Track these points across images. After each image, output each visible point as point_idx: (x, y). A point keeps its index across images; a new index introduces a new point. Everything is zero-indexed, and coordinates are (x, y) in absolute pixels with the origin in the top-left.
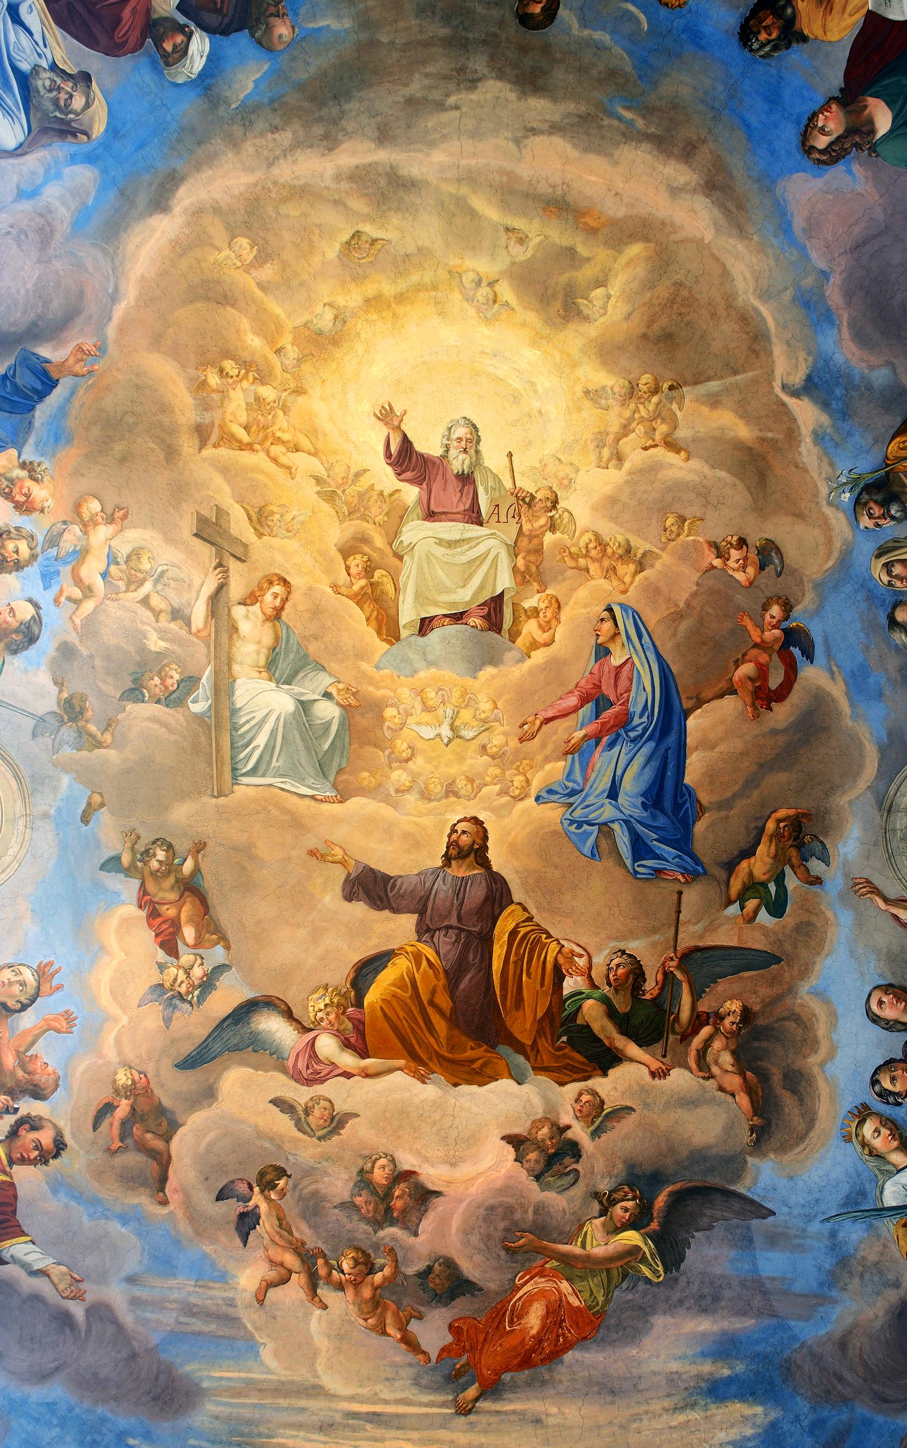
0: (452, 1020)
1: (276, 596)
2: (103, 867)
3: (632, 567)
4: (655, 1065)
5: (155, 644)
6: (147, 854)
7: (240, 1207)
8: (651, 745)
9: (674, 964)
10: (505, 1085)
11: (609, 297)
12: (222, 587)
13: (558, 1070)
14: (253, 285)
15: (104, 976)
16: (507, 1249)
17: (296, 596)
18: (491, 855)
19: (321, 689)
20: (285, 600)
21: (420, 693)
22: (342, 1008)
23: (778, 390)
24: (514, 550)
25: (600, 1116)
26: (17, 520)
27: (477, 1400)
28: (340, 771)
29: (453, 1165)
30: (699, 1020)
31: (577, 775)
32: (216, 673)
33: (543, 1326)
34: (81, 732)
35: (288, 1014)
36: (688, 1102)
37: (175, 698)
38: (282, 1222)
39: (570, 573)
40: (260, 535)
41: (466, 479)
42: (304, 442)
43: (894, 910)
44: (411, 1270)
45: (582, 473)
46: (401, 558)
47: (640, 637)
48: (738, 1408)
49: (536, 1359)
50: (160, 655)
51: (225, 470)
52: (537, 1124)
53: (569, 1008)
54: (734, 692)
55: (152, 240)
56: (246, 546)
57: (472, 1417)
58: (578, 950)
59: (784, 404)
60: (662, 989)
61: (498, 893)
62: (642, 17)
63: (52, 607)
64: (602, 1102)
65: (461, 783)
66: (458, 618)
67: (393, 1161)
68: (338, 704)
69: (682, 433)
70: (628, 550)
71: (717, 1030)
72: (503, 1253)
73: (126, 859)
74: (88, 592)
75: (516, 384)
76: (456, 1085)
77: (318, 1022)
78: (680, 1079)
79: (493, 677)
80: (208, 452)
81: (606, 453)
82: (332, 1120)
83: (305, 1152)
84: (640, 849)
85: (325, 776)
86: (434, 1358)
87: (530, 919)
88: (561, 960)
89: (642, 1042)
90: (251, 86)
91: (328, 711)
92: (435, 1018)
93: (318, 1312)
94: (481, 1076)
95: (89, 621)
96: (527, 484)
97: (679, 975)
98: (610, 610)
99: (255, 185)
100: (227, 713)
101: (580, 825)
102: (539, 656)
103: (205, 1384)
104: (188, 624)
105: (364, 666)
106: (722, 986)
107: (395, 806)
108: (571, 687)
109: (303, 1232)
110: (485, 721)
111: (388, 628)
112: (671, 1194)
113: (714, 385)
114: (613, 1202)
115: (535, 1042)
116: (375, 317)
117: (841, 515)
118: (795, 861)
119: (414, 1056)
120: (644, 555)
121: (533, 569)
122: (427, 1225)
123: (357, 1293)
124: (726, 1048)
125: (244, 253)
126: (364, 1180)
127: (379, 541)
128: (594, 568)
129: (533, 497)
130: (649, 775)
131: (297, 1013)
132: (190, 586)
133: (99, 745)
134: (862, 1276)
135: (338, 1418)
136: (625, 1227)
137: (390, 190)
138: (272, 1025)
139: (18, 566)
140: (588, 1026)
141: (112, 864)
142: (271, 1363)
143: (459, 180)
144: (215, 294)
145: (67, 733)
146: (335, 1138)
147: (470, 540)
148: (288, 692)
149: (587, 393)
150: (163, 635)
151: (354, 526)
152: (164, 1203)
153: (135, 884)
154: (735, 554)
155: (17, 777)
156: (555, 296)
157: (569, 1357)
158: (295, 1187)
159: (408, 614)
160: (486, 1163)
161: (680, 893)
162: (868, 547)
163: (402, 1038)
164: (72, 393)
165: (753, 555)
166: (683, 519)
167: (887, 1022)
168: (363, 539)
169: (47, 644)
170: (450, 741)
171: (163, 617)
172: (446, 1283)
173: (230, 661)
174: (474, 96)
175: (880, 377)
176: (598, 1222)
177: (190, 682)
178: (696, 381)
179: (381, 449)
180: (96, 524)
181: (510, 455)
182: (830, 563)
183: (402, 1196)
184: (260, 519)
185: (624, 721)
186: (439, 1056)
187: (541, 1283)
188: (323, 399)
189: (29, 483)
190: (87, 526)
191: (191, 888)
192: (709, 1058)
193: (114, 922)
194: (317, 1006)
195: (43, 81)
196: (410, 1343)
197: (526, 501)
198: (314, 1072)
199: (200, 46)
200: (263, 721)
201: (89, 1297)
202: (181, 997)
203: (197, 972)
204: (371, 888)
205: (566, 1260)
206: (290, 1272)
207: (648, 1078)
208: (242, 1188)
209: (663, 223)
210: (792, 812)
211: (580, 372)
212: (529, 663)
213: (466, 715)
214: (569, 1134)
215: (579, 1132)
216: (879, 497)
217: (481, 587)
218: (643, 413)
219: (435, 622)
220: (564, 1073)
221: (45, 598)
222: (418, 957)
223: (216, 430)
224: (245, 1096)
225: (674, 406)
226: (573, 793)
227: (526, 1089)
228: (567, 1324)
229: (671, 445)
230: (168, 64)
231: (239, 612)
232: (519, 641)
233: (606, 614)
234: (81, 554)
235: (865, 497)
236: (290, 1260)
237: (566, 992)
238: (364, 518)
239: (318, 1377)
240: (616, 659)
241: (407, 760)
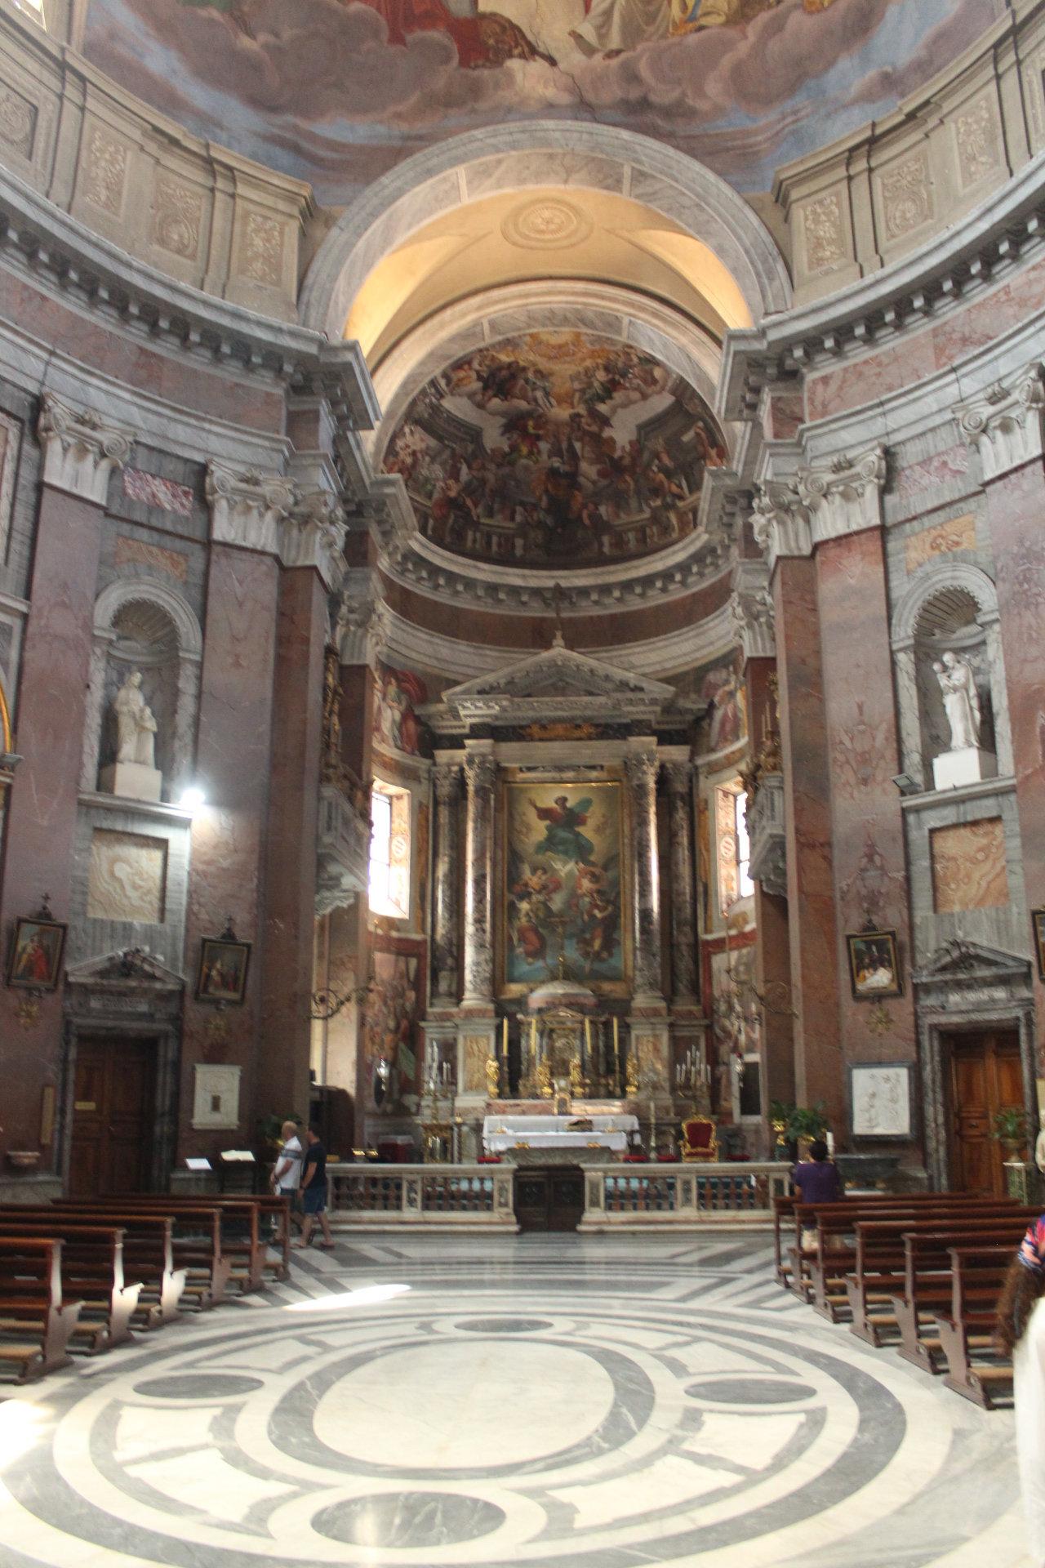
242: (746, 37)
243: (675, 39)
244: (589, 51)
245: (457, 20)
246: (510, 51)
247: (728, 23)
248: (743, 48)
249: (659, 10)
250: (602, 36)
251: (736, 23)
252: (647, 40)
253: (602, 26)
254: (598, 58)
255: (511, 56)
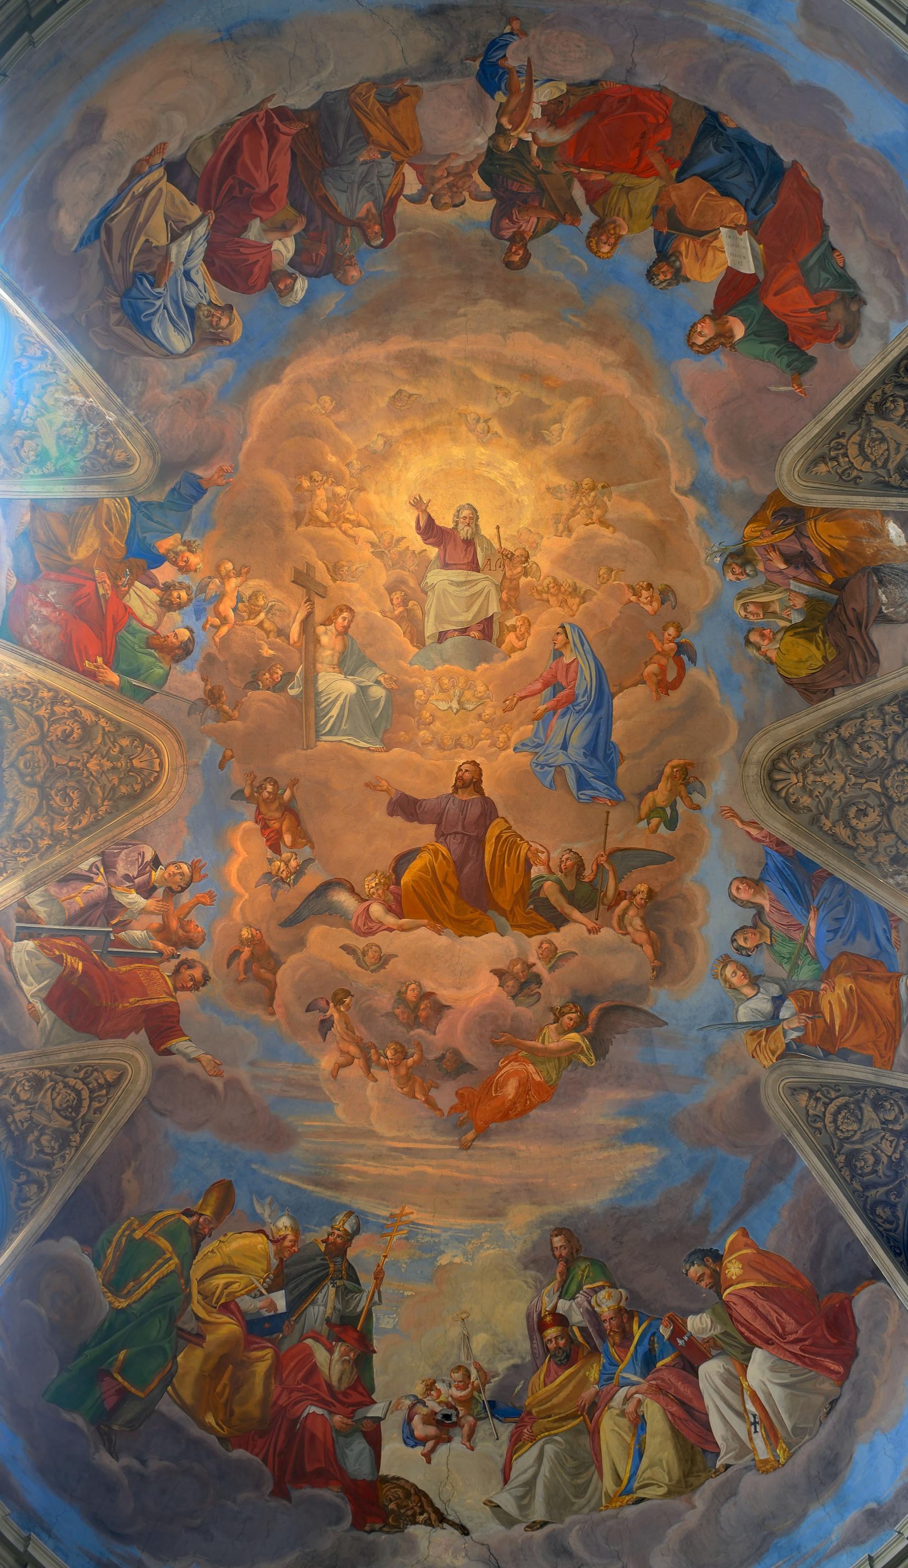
0: (458, 894)
1: (344, 619)
2: (233, 797)
3: (577, 600)
4: (591, 925)
5: (267, 652)
6: (261, 788)
7: (321, 1016)
8: (590, 715)
9: (604, 858)
10: (493, 936)
11: (563, 430)
12: (310, 615)
13: (527, 927)
14: (332, 424)
15: (234, 868)
16: (494, 1044)
17: (358, 618)
18: (484, 786)
19: (373, 678)
20: (350, 622)
21: (438, 680)
22: (386, 886)
23: (673, 490)
24: (500, 588)
25: (554, 958)
26: (180, 578)
27: (473, 1140)
28: (386, 731)
29: (459, 989)
30: (620, 896)
31: (541, 734)
32: (306, 670)
33: (517, 1093)
34: (219, 711)
35: (352, 890)
36: (611, 950)
37: (279, 687)
38: (348, 1027)
39: (537, 603)
40: (335, 580)
41: (469, 543)
42: (364, 520)
43: (747, 829)
44: (431, 1057)
45: (545, 539)
46: (426, 593)
47: (583, 645)
48: (642, 1149)
49: (512, 1113)
50: (269, 659)
51: (312, 540)
52: (513, 963)
53: (535, 886)
54: (644, 682)
55: (269, 400)
56: (325, 588)
57: (470, 1151)
58: (541, 848)
59: (677, 500)
60: (596, 875)
61: (489, 811)
62: (584, 264)
63: (201, 632)
64: (556, 949)
65: (465, 739)
66: (464, 631)
67: (420, 985)
68: (385, 688)
69: (610, 516)
70: (575, 589)
71: (631, 903)
72: (491, 1046)
73: (247, 791)
74: (224, 620)
75: (502, 482)
76: (460, 936)
77: (370, 896)
78: (607, 934)
79: (486, 669)
80: (302, 529)
81: (561, 527)
82: (381, 958)
83: (364, 979)
84: (582, 783)
85: (376, 735)
86: (446, 1114)
87: (510, 828)
88: (530, 855)
89: (583, 910)
90: (333, 306)
91: (378, 692)
92: (447, 892)
93: (371, 1084)
94: (477, 930)
95: (225, 639)
96: (509, 546)
97: (607, 866)
98: (563, 627)
99: (335, 364)
100: (312, 695)
101: (542, 767)
102: (516, 657)
103: (299, 1130)
104: (288, 638)
105: (402, 662)
106: (635, 874)
107: (422, 754)
108: (537, 676)
109: (362, 1032)
110: (480, 698)
111: (418, 639)
112: (600, 1010)
113: (631, 486)
114: (563, 1014)
115: (512, 909)
116: (410, 442)
117: (714, 572)
118: (683, 794)
119: (433, 917)
120: (585, 592)
121: (513, 600)
122: (441, 1027)
123: (397, 1071)
124: (637, 915)
125: (327, 405)
126: (400, 997)
127: (412, 583)
128: (552, 600)
129: (513, 554)
130: (588, 735)
131: (357, 889)
132: (289, 614)
133: (231, 718)
134: (723, 1066)
135: (384, 1151)
136: (570, 1030)
137: (421, 365)
138: (343, 898)
139: (180, 606)
140: (547, 899)
141: (239, 795)
142: (342, 1115)
143: (466, 358)
144: (307, 431)
145: (210, 712)
146: (382, 971)
147: (472, 581)
148: (352, 681)
149: (548, 489)
150: (272, 646)
151: (397, 572)
152: (273, 1014)
153: (253, 807)
154: (645, 593)
155: (178, 741)
156: (527, 428)
157: (533, 1113)
158: (356, 1002)
159: (430, 629)
160: (482, 986)
161: (608, 813)
162: (732, 593)
163: (426, 907)
164: (216, 496)
165: (656, 594)
166: (611, 570)
167: (742, 901)
168: (403, 582)
169: (198, 655)
170: (458, 711)
171: (271, 635)
172: (454, 1065)
173: (315, 661)
174: (476, 309)
175: (739, 486)
176: (553, 1027)
177: (289, 676)
178: (620, 484)
179: (413, 524)
180: (230, 577)
181: (498, 527)
182: (707, 602)
183: (426, 1009)
184: (335, 571)
185: (572, 699)
186: (450, 917)
187: (515, 1066)
188: (377, 493)
189: (188, 554)
190: (224, 578)
191: (289, 809)
192: (626, 922)
193: (240, 833)
194: (371, 884)
195: (205, 310)
196: (431, 1103)
197: (508, 557)
198: (368, 927)
199: (301, 285)
200: (336, 699)
201: (225, 1075)
202: (283, 880)
203: (293, 863)
204: (406, 807)
205: (532, 1051)
206: (353, 1058)
207: (586, 934)
208: (322, 1004)
209: (598, 385)
210: (682, 762)
211: (543, 476)
212: (509, 661)
213: (468, 694)
214: (534, 969)
215: (541, 968)
216: (739, 561)
217: (478, 612)
218: (585, 502)
219: (449, 635)
220: (531, 929)
221: (197, 626)
222: (436, 853)
223: (307, 515)
224: (324, 942)
225: (605, 499)
226: (538, 746)
227: (507, 939)
228: (532, 1092)
229: (603, 522)
230: (281, 296)
231: (321, 629)
232: (503, 646)
233: (560, 630)
234: (220, 597)
235: (730, 561)
236: (353, 1050)
237: (532, 876)
238: (402, 568)
239: (371, 1125)
240: (567, 660)
241: (430, 724)
242: (694, 1507)
243: (610, 1512)
244: (508, 1521)
245: (355, 1481)
246: (414, 1515)
247: (669, 1494)
248: (691, 1519)
249: (589, 1481)
250: (522, 1508)
251: (680, 1494)
252: (576, 1513)
253: (523, 1497)
254: (519, 1529)
255: (415, 1523)
